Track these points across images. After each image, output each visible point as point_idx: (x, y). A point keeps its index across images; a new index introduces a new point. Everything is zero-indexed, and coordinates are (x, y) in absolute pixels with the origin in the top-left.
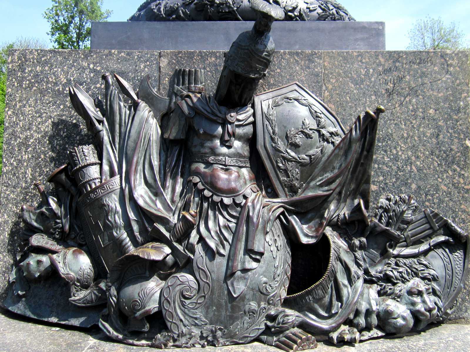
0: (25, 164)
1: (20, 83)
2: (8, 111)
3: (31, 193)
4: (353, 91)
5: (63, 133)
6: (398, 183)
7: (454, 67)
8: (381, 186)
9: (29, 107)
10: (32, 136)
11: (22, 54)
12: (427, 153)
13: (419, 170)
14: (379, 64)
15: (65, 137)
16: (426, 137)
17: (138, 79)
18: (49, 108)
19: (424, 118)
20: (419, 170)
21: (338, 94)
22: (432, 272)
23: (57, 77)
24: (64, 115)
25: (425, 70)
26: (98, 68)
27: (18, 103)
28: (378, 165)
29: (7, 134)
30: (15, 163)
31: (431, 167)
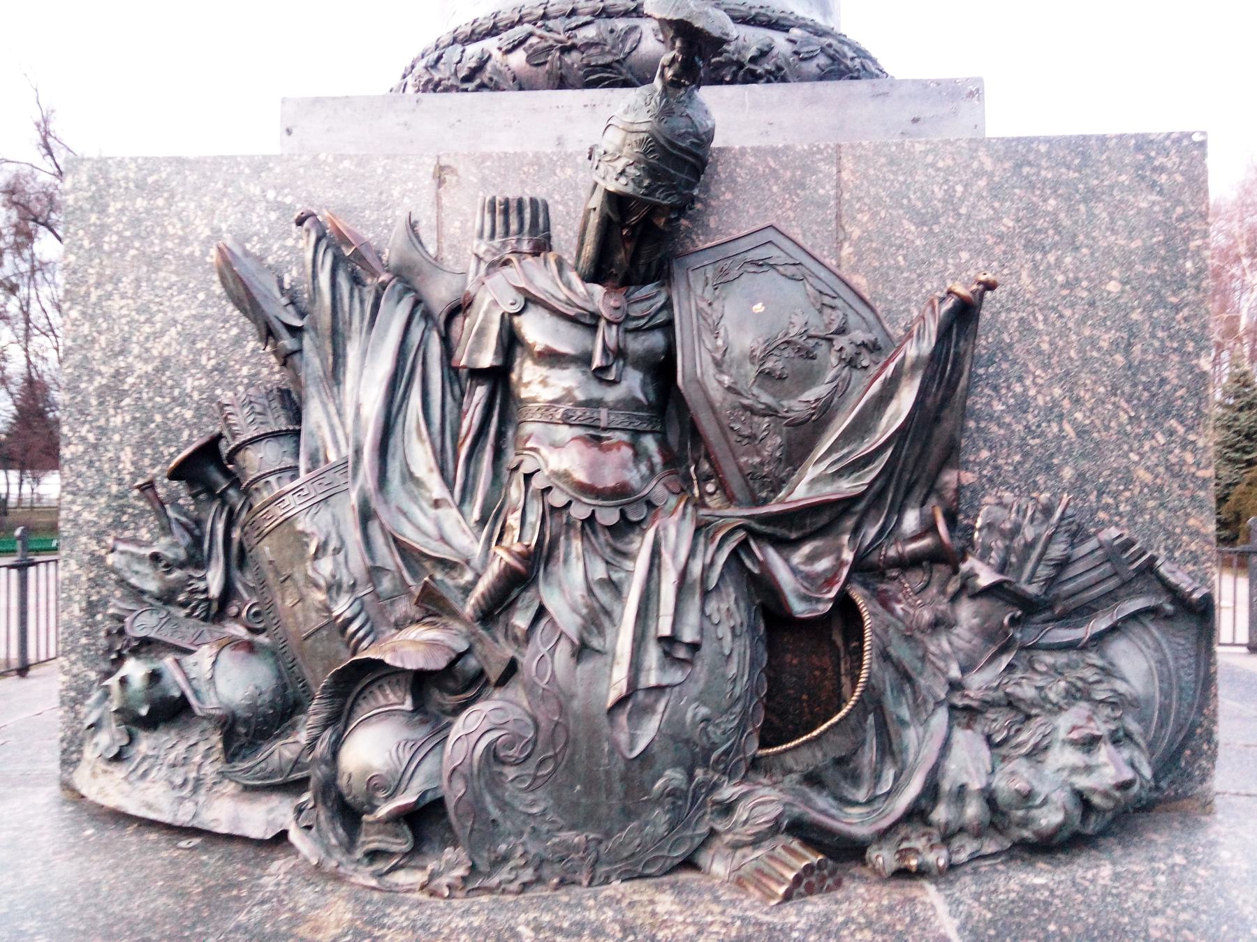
1: (97, 238)
2: (70, 309)
4: (913, 242)
5: (209, 359)
6: (1027, 466)
7: (1170, 174)
8: (985, 472)
10: (130, 370)
11: (100, 169)
12: (1102, 390)
13: (1081, 432)
15: (212, 371)
16: (1099, 349)
17: (387, 225)
18: (169, 300)
19: (1092, 304)
20: (1081, 432)
21: (875, 250)
22: (1121, 687)
23: (186, 224)
24: (207, 316)
25: (1096, 182)
26: (288, 200)
27: (92, 289)
28: (977, 422)
31: (1113, 424)
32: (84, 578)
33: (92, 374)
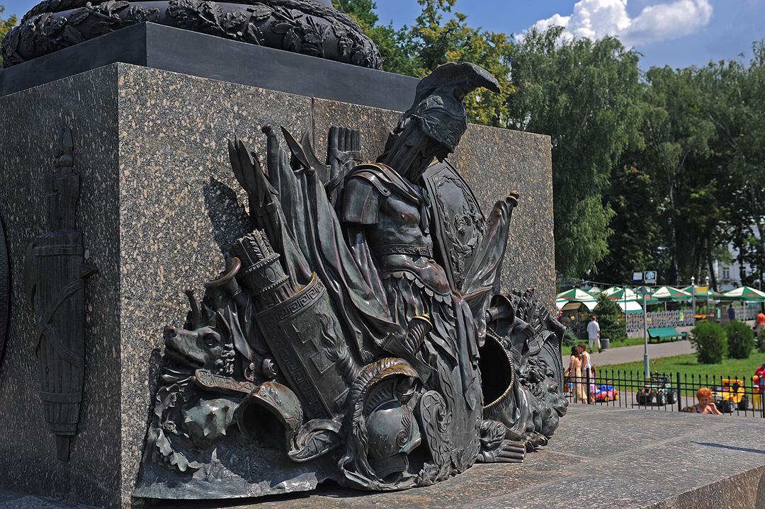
0: (155, 259)
1: (140, 122)
2: (124, 169)
3: (166, 307)
9: (156, 165)
11: (140, 75)
14: (495, 144)
18: (183, 169)
26: (245, 113)
29: (125, 209)
30: (139, 257)
32: (136, 357)
33: (140, 215)
